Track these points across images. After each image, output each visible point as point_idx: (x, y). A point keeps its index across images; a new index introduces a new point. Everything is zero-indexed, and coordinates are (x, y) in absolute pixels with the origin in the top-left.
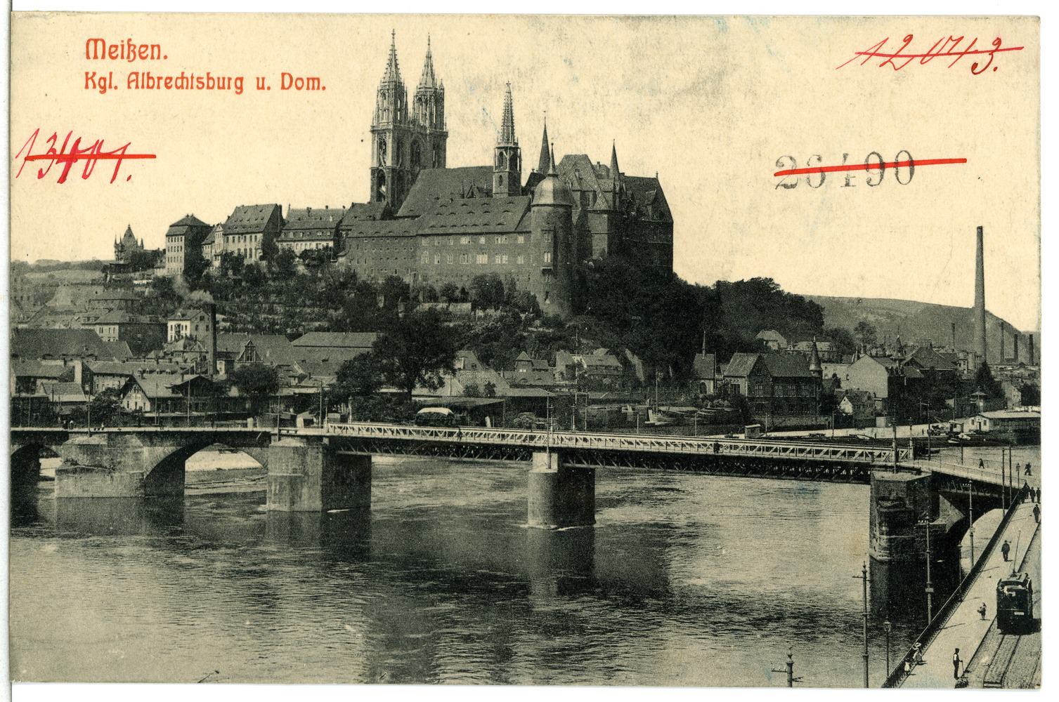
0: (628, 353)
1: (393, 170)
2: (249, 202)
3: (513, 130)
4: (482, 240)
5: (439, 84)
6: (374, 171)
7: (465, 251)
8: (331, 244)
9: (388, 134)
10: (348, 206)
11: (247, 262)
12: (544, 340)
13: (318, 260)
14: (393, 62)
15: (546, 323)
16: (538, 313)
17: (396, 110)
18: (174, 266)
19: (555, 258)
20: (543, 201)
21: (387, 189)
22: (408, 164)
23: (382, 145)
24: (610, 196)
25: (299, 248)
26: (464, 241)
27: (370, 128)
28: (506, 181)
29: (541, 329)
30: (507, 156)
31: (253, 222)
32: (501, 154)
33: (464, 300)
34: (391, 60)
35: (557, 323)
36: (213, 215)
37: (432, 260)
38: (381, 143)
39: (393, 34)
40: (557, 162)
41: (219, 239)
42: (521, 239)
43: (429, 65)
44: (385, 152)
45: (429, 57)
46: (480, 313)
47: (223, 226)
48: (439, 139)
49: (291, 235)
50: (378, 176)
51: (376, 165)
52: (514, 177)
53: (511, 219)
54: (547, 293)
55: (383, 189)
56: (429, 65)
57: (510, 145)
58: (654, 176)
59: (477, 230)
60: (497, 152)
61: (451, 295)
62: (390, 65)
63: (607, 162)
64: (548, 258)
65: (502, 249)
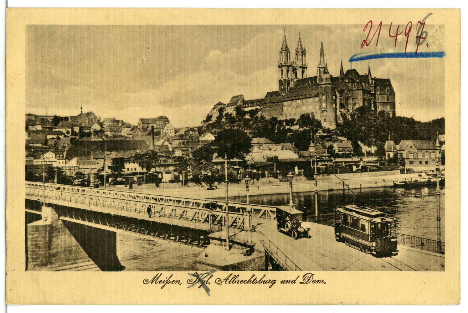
0: (359, 142)
5: (304, 49)
11: (232, 116)
12: (322, 137)
13: (252, 113)
14: (285, 40)
15: (324, 131)
16: (321, 127)
18: (214, 119)
25: (247, 109)
27: (278, 66)
29: (321, 134)
30: (322, 70)
32: (320, 70)
33: (296, 124)
35: (328, 131)
36: (226, 101)
40: (344, 73)
42: (317, 99)
45: (300, 39)
46: (301, 129)
48: (304, 68)
57: (324, 66)
60: (319, 69)
61: (291, 122)
63: (367, 74)
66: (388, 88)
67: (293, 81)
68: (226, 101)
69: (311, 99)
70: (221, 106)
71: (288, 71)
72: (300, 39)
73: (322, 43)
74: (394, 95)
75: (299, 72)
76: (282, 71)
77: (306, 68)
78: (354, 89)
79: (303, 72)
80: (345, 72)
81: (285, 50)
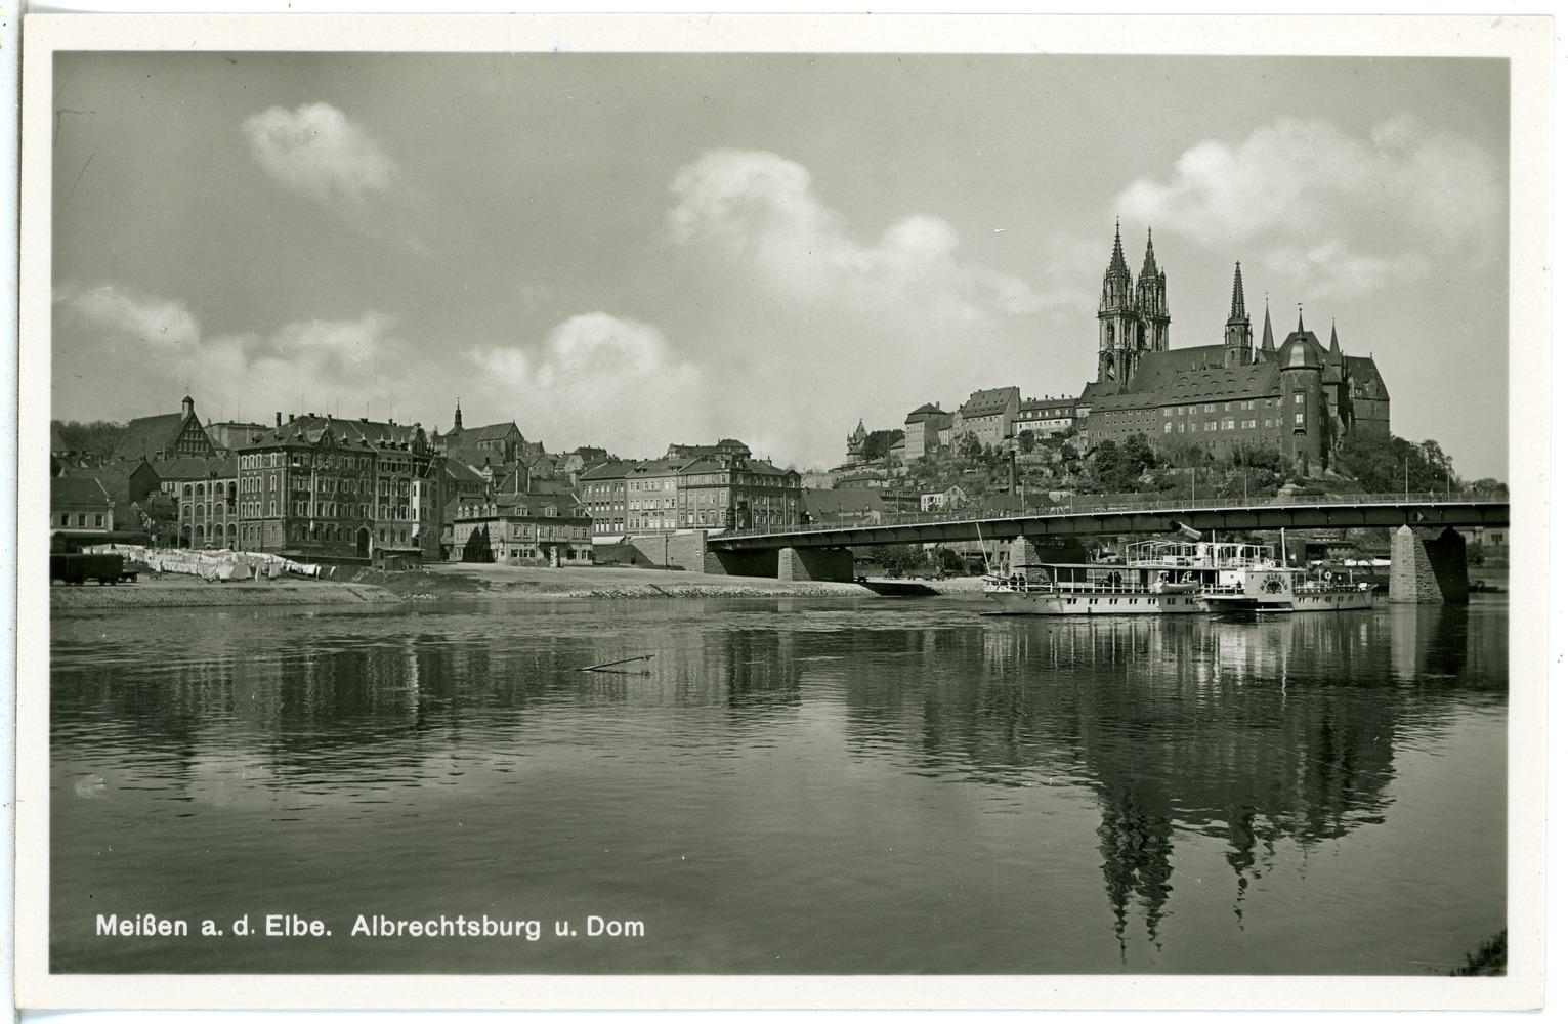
1: (1122, 352)
3: (1243, 307)
4: (1227, 406)
5: (1159, 274)
6: (1102, 354)
7: (1210, 418)
8: (1070, 421)
9: (1116, 319)
17: (1123, 297)
20: (1292, 364)
21: (1116, 372)
23: (1111, 328)
24: (1338, 369)
26: (1210, 409)
28: (1237, 357)
31: (991, 404)
34: (1116, 249)
38: (1108, 328)
39: (1118, 225)
41: (958, 424)
43: (1150, 257)
45: (1150, 245)
48: (1162, 322)
49: (1029, 415)
50: (1107, 359)
51: (1103, 349)
52: (1246, 350)
53: (1258, 387)
54: (1300, 452)
55: (1112, 371)
56: (1150, 257)
58: (1368, 356)
59: (1218, 398)
64: (1299, 418)
66: (1373, 382)
67: (1139, 358)
69: (1251, 403)
72: (1150, 245)
73: (1238, 264)
74: (1388, 400)
75: (1149, 333)
76: (1111, 328)
77: (1167, 321)
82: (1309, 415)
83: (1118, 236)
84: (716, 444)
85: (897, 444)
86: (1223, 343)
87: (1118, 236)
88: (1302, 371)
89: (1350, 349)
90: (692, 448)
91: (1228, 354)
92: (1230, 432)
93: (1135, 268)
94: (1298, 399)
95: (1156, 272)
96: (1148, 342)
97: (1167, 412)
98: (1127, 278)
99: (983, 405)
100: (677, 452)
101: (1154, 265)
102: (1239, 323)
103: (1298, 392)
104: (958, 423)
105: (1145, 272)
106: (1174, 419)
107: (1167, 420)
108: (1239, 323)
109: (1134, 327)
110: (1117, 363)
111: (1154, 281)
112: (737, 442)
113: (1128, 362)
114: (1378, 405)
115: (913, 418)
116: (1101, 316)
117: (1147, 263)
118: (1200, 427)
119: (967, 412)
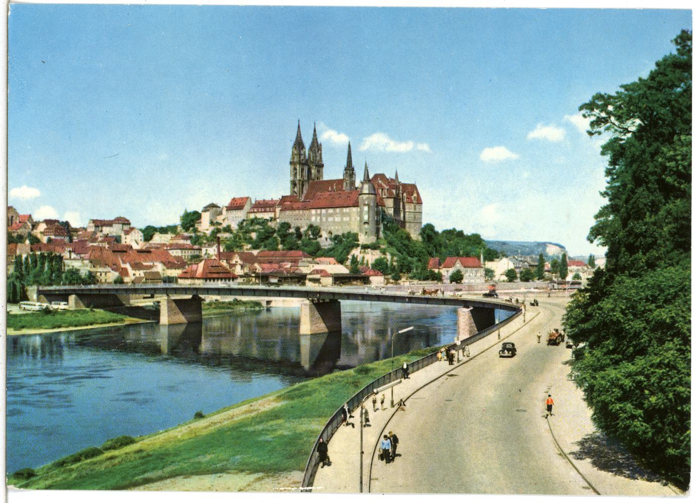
1: (300, 180)
2: (237, 196)
4: (338, 210)
5: (319, 143)
6: (291, 181)
7: (331, 215)
10: (281, 198)
17: (300, 155)
19: (369, 218)
22: (306, 178)
23: (295, 169)
24: (394, 191)
26: (331, 211)
27: (289, 163)
28: (348, 185)
31: (238, 205)
37: (316, 219)
43: (315, 135)
44: (296, 173)
47: (226, 207)
48: (320, 166)
50: (294, 184)
51: (292, 178)
52: (352, 183)
54: (366, 233)
56: (315, 135)
62: (298, 135)
63: (394, 178)
64: (366, 218)
65: (348, 214)
66: (415, 195)
68: (224, 201)
70: (214, 209)
71: (302, 170)
72: (315, 131)
74: (422, 203)
75: (313, 171)
76: (295, 169)
77: (322, 166)
78: (384, 196)
79: (319, 171)
80: (371, 176)
81: (299, 144)
82: (371, 216)
83: (299, 126)
84: (112, 218)
85: (198, 221)
86: (341, 177)
87: (299, 126)
88: (367, 195)
89: (403, 180)
90: (101, 221)
91: (345, 184)
92: (339, 223)
93: (307, 142)
94: (366, 208)
95: (317, 143)
96: (313, 175)
97: (313, 211)
98: (303, 147)
99: (235, 205)
100: (93, 222)
101: (316, 139)
102: (350, 170)
103: (365, 205)
104: (224, 212)
105: (313, 143)
106: (317, 215)
107: (312, 215)
108: (350, 170)
109: (306, 168)
110: (298, 185)
111: (316, 146)
112: (124, 218)
113: (303, 185)
114: (417, 207)
115: (206, 209)
116: (291, 163)
117: (313, 139)
118: (327, 219)
119: (230, 208)
